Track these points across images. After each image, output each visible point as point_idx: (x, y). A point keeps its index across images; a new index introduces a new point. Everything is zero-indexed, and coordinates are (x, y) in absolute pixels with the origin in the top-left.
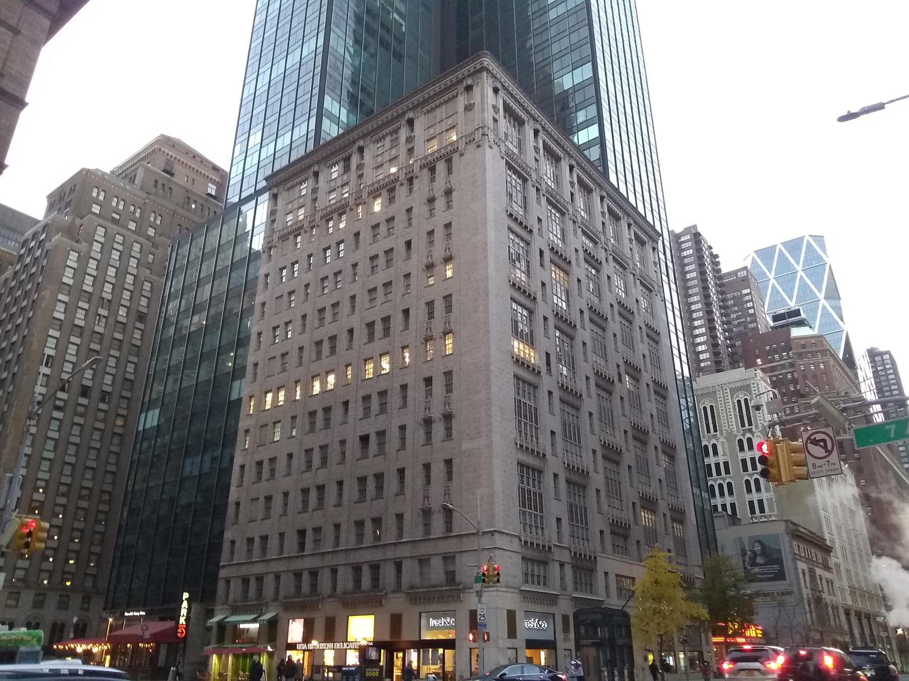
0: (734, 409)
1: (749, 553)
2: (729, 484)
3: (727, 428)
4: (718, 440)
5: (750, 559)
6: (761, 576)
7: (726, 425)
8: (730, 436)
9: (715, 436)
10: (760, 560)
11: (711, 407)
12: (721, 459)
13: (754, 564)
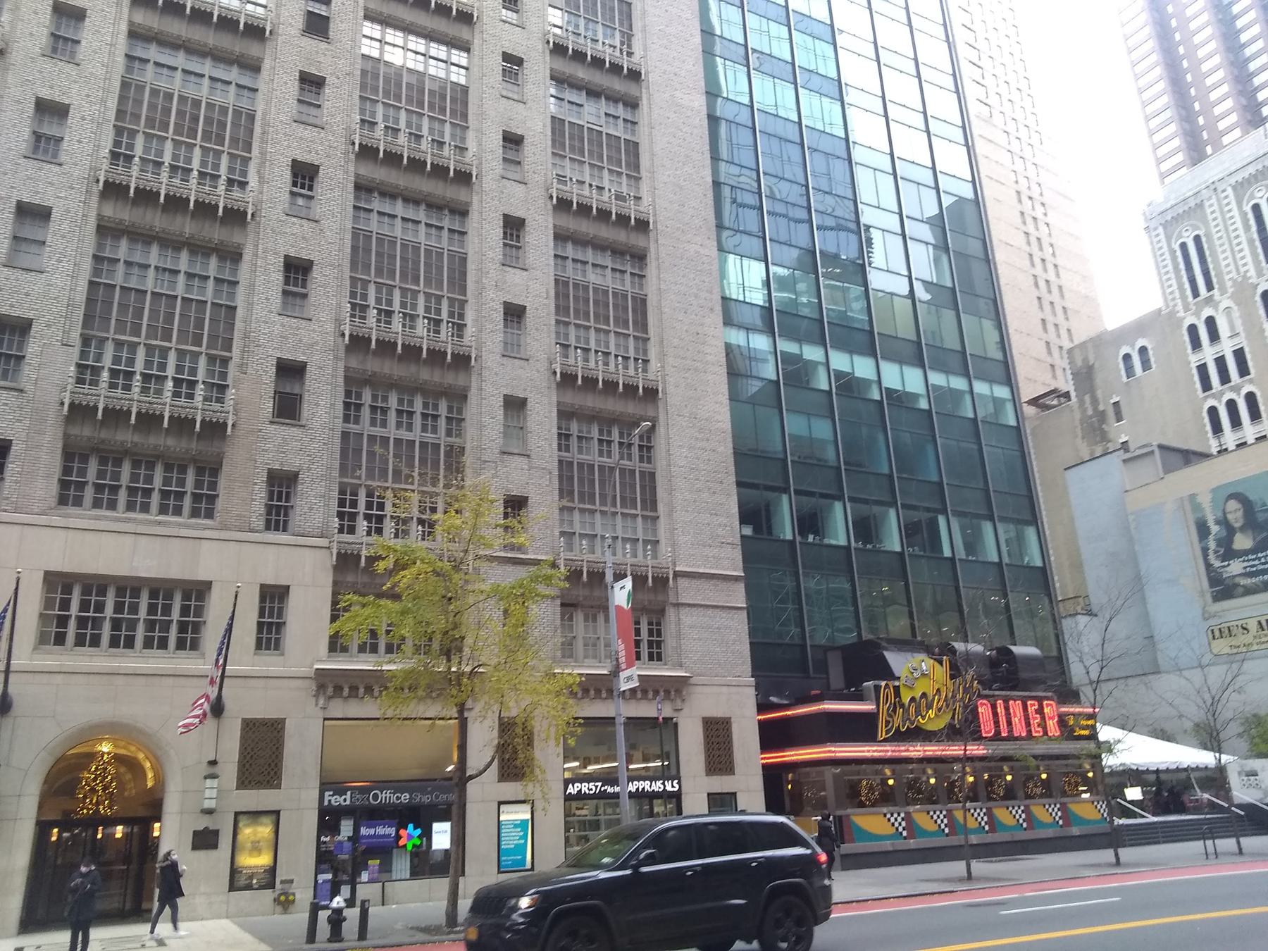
0: (1247, 227)
1: (1215, 529)
2: (1251, 399)
3: (1234, 275)
4: (1216, 307)
5: (1219, 542)
6: (1254, 580)
7: (1232, 267)
8: (1243, 287)
9: (1209, 301)
10: (1242, 542)
11: (1197, 239)
12: (1227, 347)
13: (1229, 554)
